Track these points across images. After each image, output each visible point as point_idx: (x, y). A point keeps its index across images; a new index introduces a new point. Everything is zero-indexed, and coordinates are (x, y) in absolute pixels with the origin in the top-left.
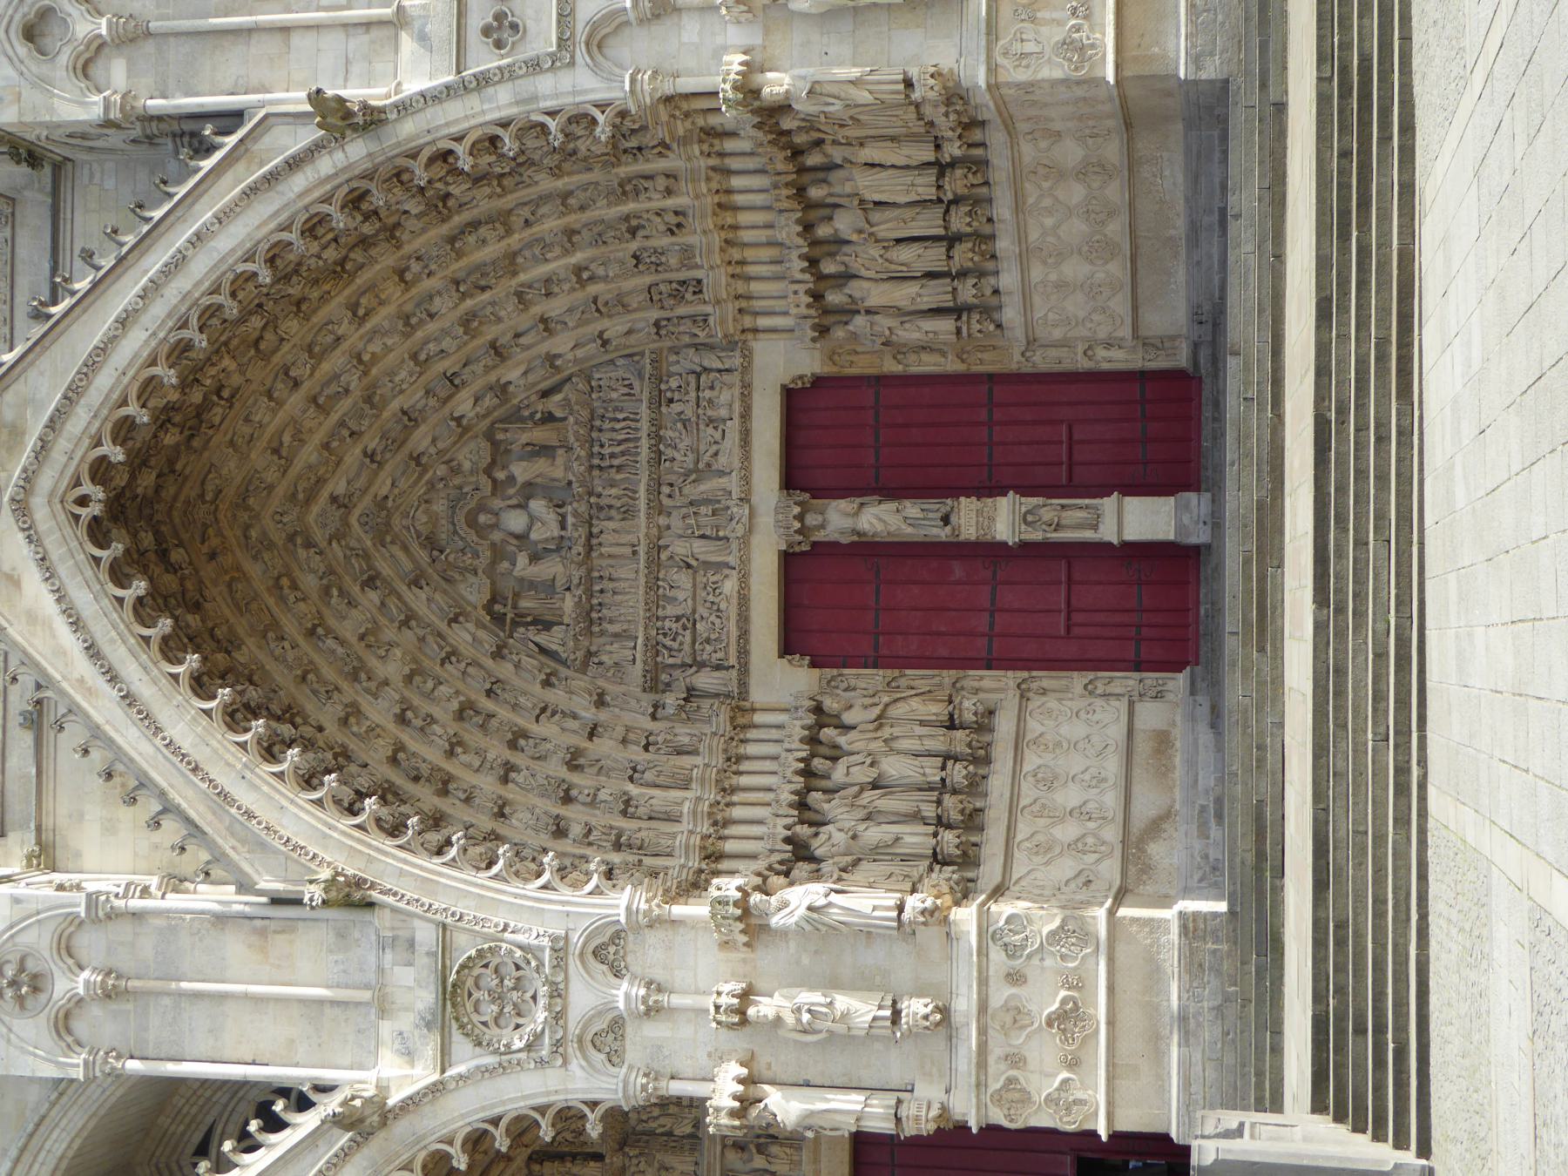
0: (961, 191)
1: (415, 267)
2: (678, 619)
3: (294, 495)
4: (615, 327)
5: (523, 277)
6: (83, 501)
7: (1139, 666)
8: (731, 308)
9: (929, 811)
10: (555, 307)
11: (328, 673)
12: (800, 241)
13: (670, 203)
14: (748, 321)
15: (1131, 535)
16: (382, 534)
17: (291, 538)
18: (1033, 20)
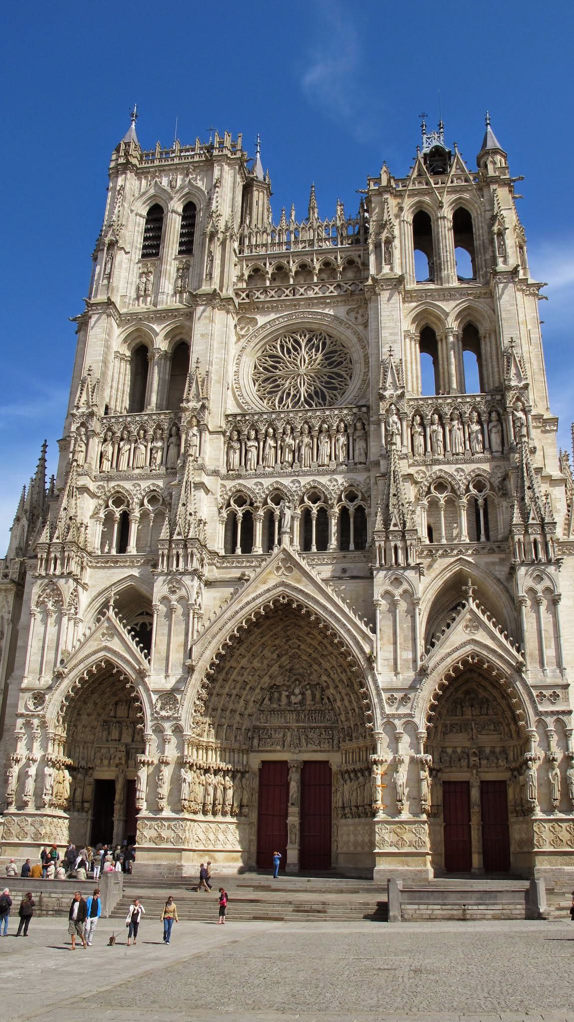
4: (343, 717)
7: (259, 853)
11: (254, 649)
15: (288, 852)
16: (292, 657)
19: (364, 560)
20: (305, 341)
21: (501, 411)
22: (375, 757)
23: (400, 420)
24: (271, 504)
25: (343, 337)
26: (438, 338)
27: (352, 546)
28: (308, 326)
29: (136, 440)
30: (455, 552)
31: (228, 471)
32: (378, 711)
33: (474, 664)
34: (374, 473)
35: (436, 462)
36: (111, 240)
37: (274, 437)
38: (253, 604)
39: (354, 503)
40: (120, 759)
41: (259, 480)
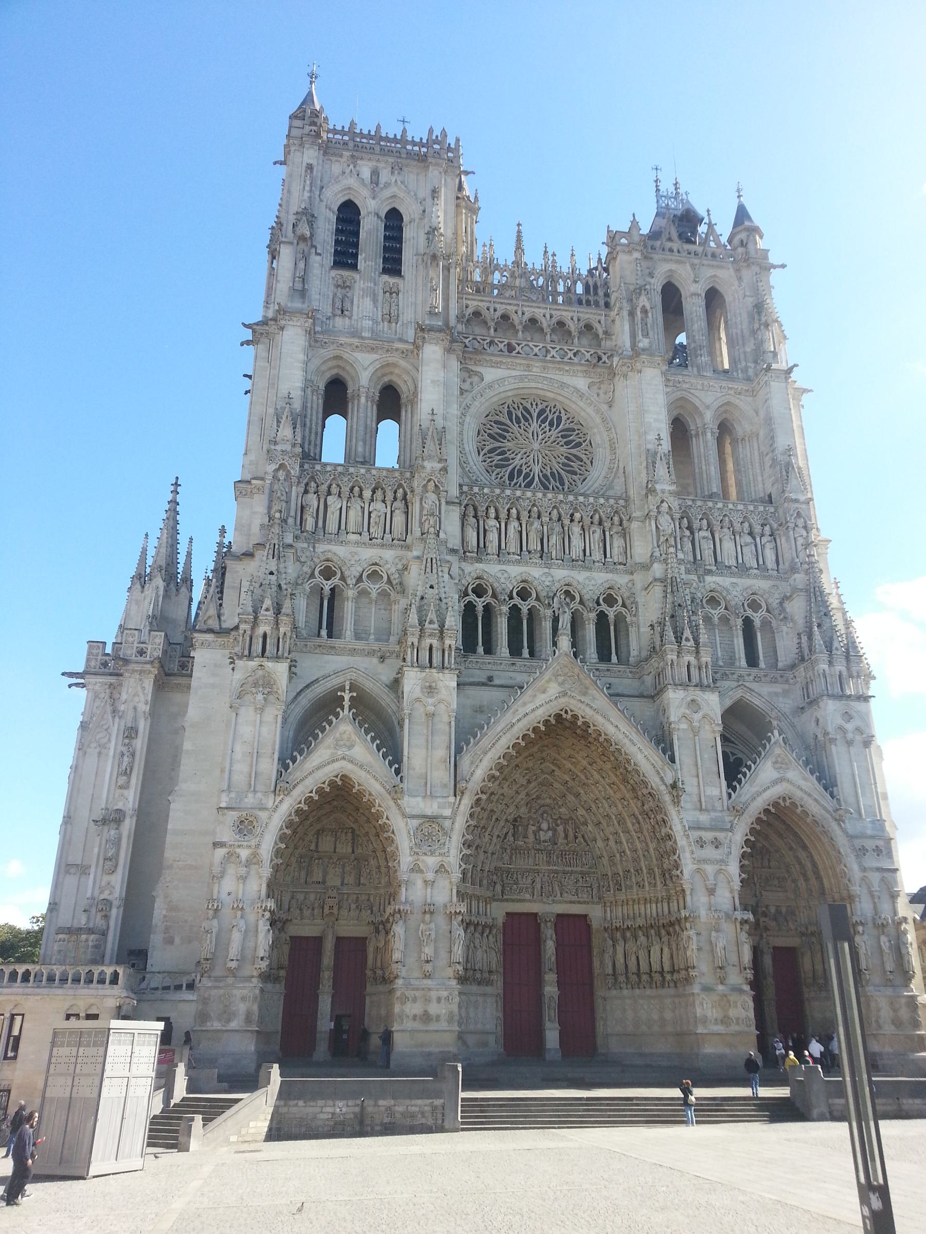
0: (655, 979)
1: (626, 803)
2: (517, 879)
3: (555, 760)
4: (605, 861)
5: (622, 834)
6: (566, 712)
8: (612, 899)
9: (469, 966)
10: (612, 843)
12: (637, 925)
13: (646, 883)
14: (608, 904)
15: (547, 1032)
17: (543, 758)
18: (712, 1007)
19: (630, 675)
20: (537, 411)
21: (775, 526)
22: (683, 913)
23: (672, 519)
24: (517, 600)
25: (583, 414)
26: (692, 432)
27: (614, 658)
28: (541, 393)
29: (350, 497)
30: (735, 676)
31: (464, 553)
32: (688, 855)
33: (785, 807)
34: (640, 579)
35: (709, 572)
36: (303, 235)
37: (518, 518)
38: (531, 717)
39: (614, 609)
40: (331, 908)
41: (504, 567)
